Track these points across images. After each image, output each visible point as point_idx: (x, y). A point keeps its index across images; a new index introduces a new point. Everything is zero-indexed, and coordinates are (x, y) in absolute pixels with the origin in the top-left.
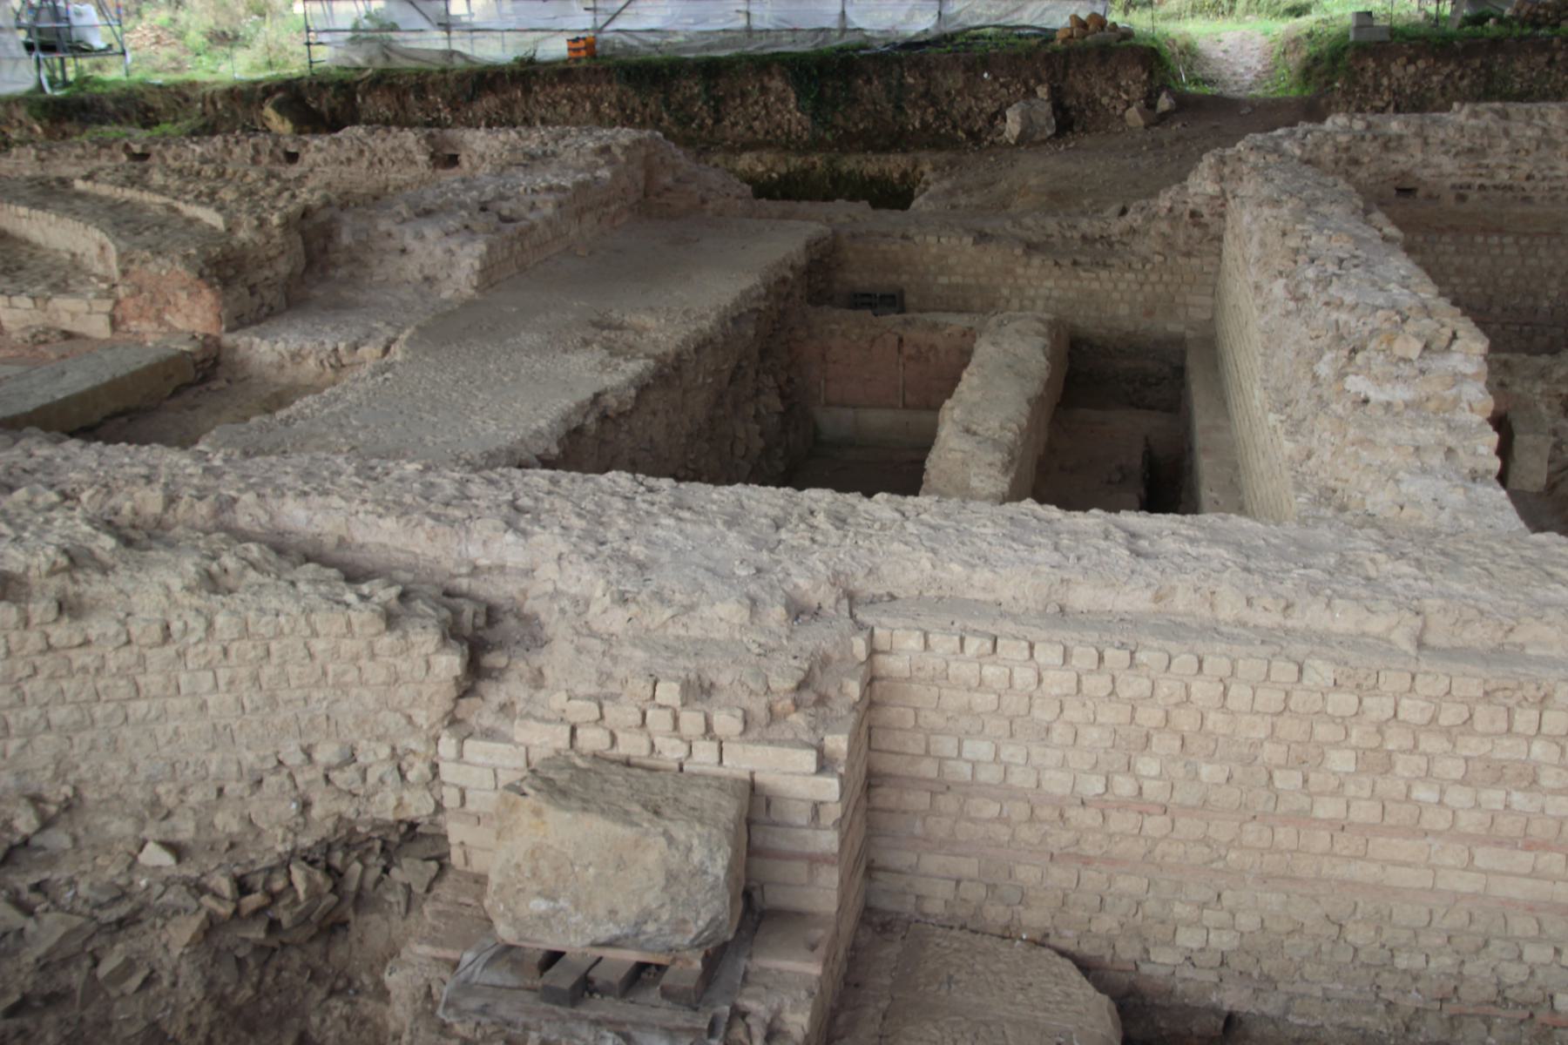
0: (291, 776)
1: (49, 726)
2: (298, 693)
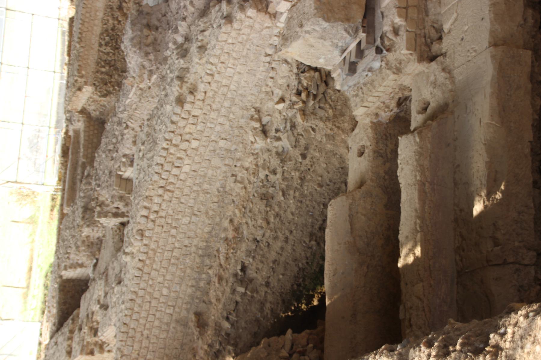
0: (274, 61)
1: (230, 108)
2: (245, 51)
